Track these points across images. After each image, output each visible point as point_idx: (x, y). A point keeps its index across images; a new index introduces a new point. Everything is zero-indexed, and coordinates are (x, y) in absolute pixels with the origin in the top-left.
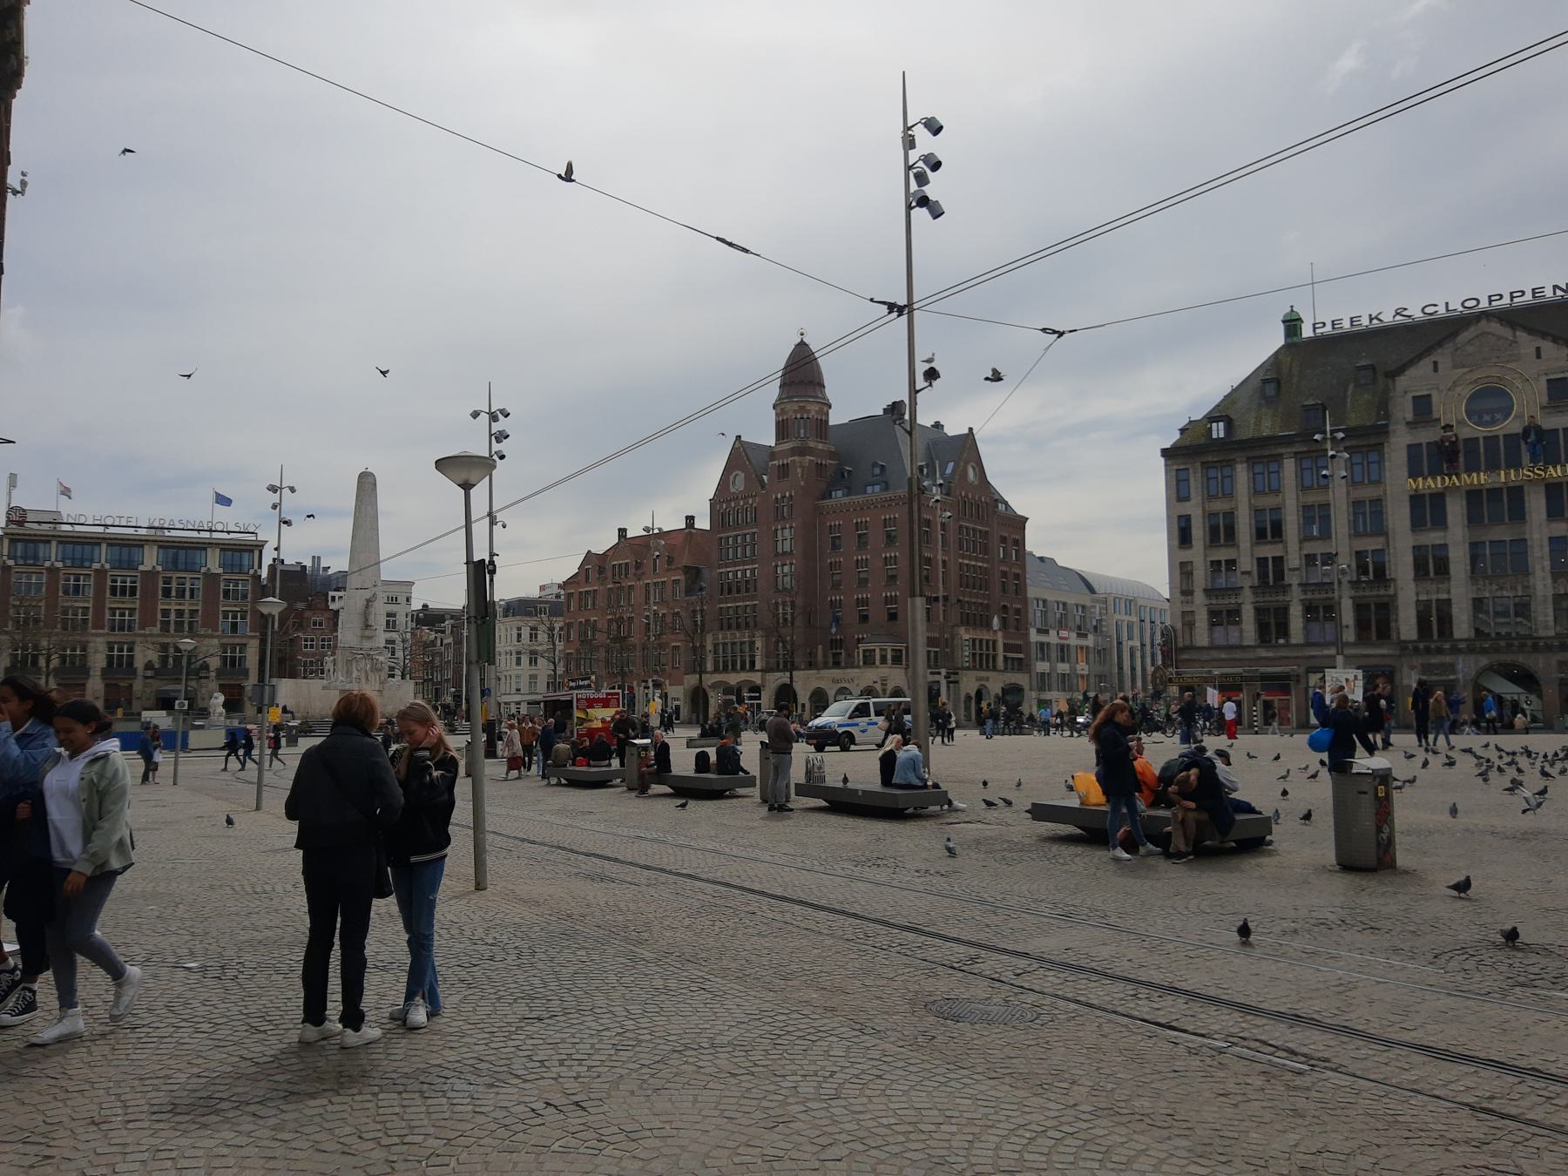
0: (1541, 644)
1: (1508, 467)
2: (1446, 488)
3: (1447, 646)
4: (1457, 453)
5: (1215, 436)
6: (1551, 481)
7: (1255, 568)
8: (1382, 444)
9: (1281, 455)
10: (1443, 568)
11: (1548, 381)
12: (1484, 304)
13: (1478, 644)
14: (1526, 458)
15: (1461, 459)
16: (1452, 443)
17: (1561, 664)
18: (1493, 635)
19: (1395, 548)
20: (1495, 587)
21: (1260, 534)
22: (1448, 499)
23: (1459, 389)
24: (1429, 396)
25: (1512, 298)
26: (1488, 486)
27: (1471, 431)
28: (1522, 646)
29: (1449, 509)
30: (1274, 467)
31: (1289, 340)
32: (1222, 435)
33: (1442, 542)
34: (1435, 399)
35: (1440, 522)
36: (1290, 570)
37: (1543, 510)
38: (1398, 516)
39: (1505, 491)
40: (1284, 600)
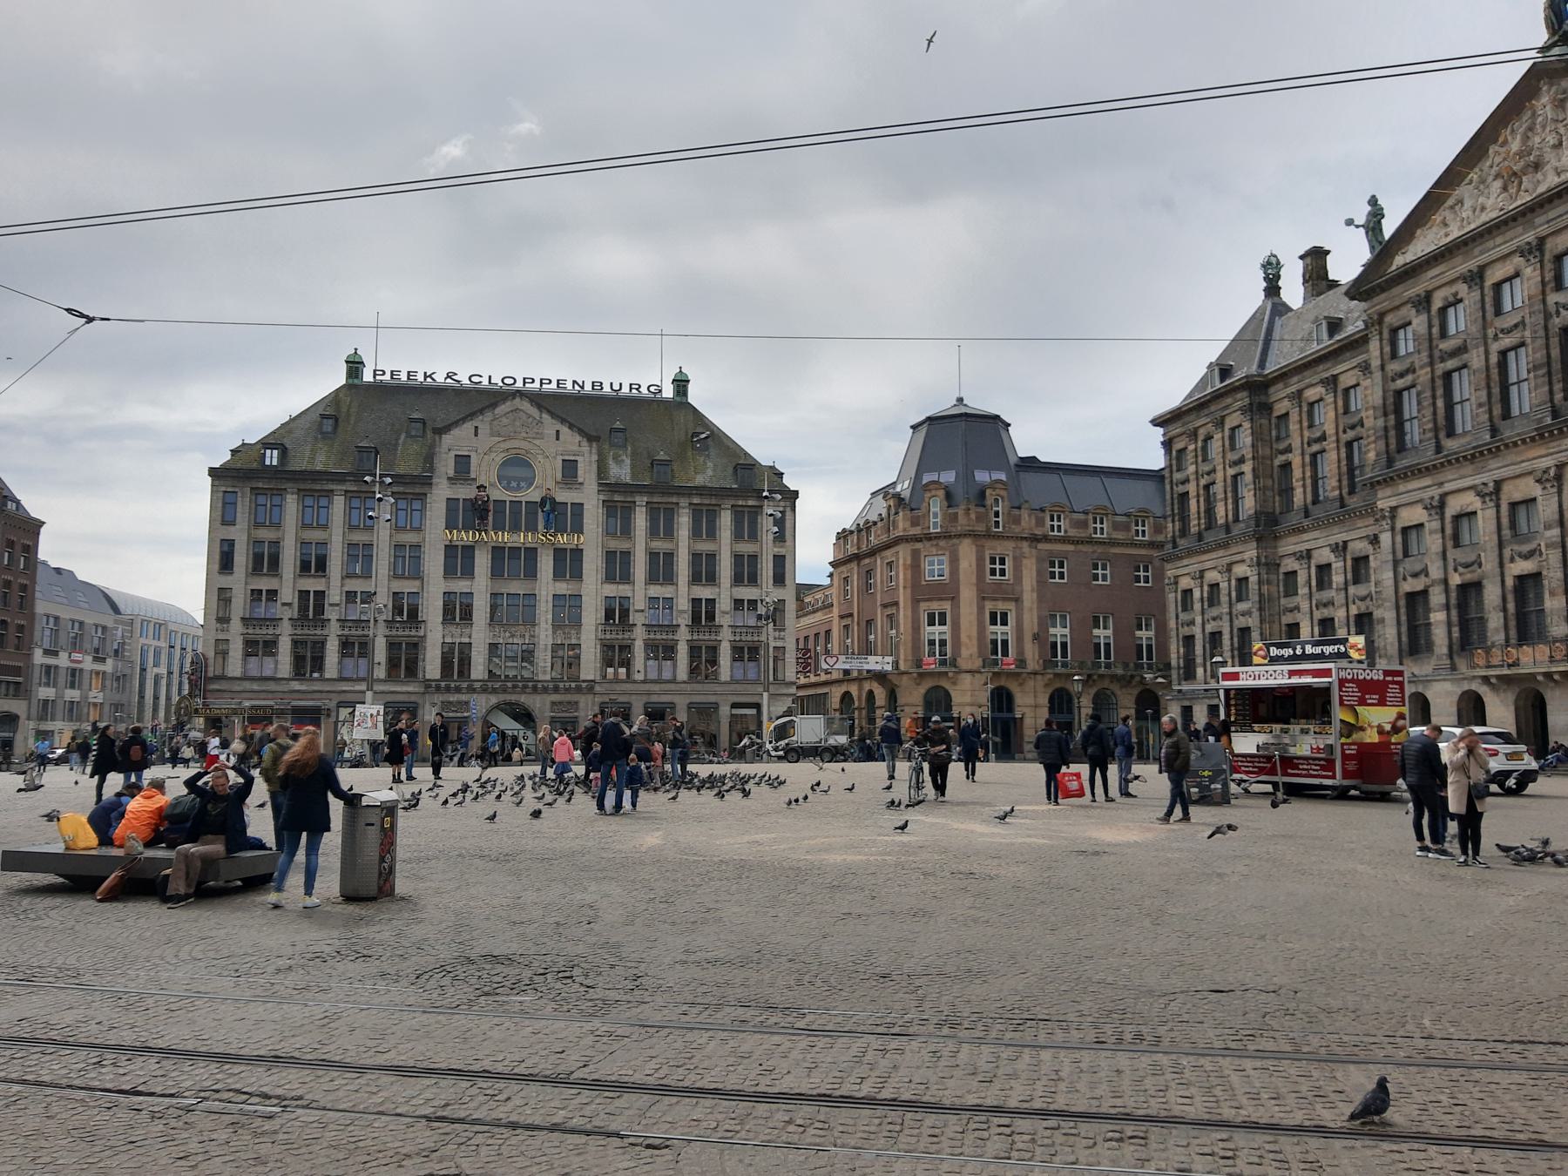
0: (540, 685)
1: (527, 530)
3: (465, 685)
4: (488, 511)
5: (268, 462)
7: (296, 600)
8: (426, 494)
9: (332, 491)
10: (467, 614)
11: (563, 460)
12: (519, 384)
13: (490, 684)
14: (541, 526)
15: (490, 518)
16: (483, 501)
17: (553, 703)
18: (503, 677)
19: (428, 592)
20: (507, 634)
21: (305, 567)
22: (477, 552)
23: (493, 455)
25: (541, 384)
26: (509, 545)
27: (497, 494)
28: (525, 687)
29: (477, 561)
30: (323, 502)
31: (350, 381)
32: (275, 463)
33: (469, 591)
34: (474, 461)
35: (469, 572)
36: (331, 605)
37: (551, 571)
38: (434, 562)
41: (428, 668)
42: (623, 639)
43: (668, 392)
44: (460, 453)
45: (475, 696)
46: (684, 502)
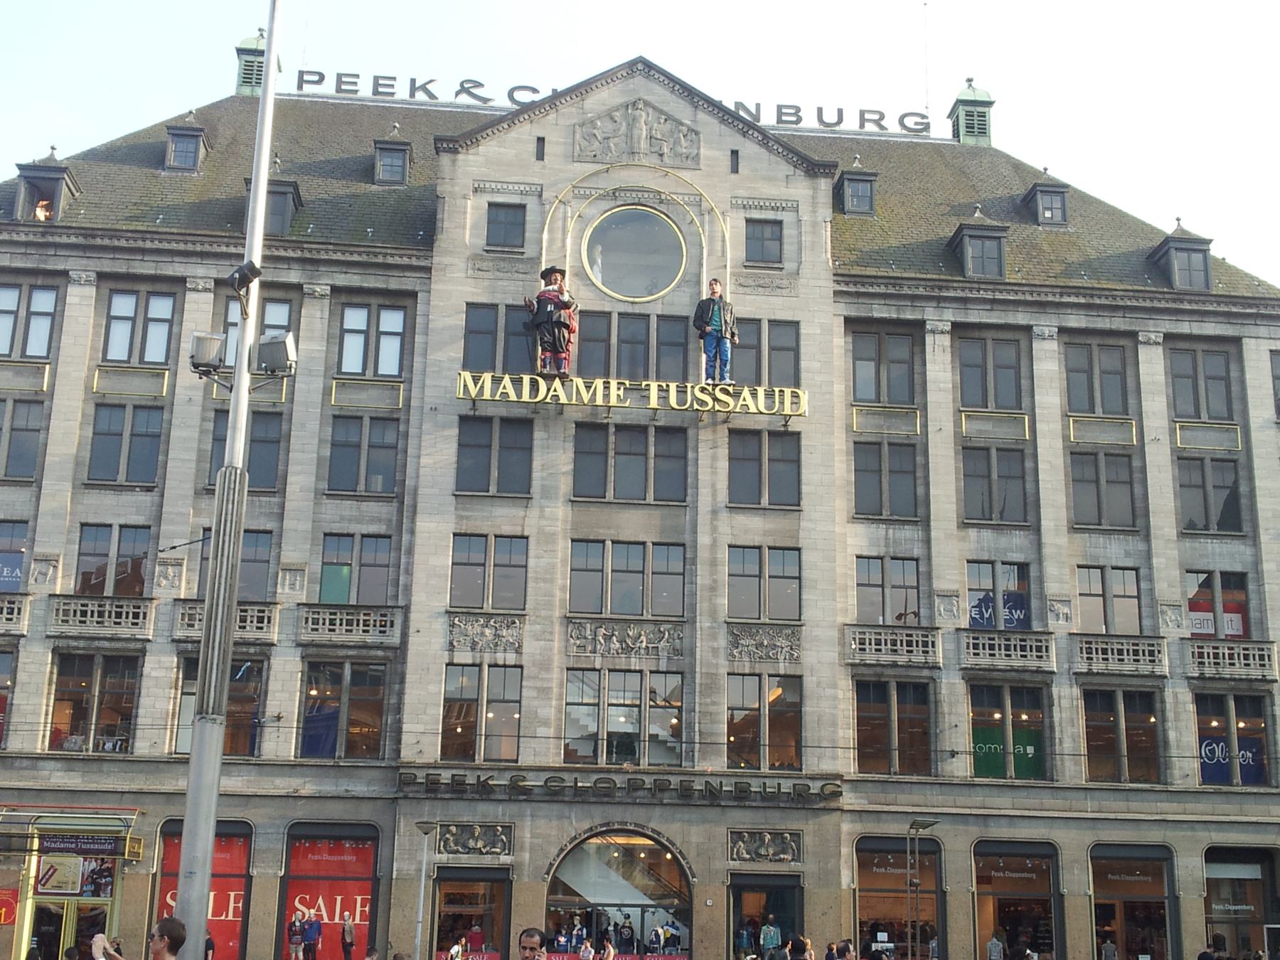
2: (537, 407)
6: (740, 423)
8: (413, 295)
9: (182, 280)
11: (748, 221)
13: (568, 779)
22: (538, 435)
24: (522, 207)
26: (616, 418)
39: (652, 431)
40: (133, 639)
41: (410, 727)
42: (909, 666)
43: (941, 130)
44: (499, 199)
45: (528, 809)
46: (1046, 324)
